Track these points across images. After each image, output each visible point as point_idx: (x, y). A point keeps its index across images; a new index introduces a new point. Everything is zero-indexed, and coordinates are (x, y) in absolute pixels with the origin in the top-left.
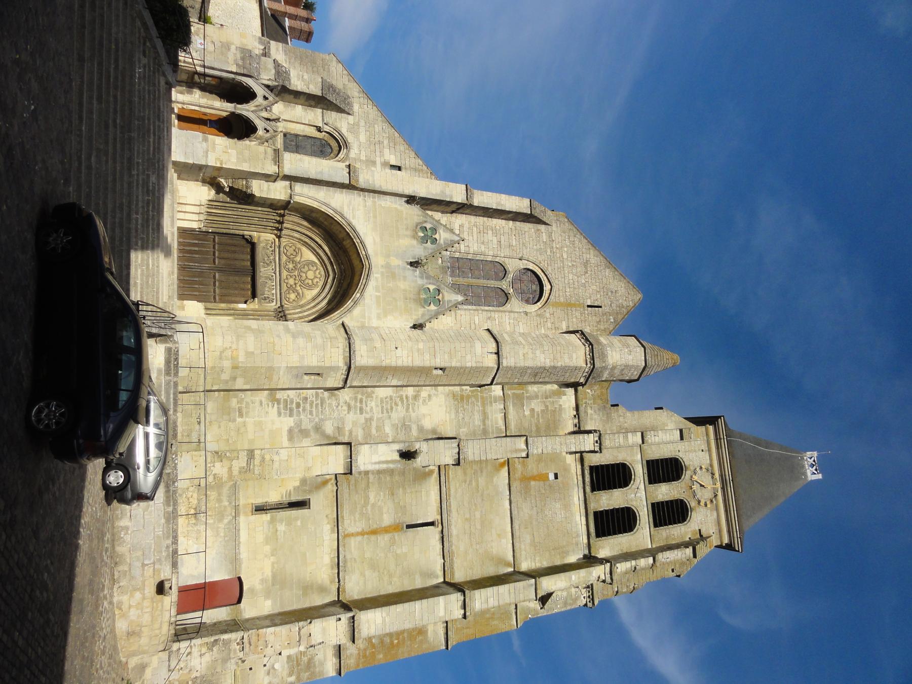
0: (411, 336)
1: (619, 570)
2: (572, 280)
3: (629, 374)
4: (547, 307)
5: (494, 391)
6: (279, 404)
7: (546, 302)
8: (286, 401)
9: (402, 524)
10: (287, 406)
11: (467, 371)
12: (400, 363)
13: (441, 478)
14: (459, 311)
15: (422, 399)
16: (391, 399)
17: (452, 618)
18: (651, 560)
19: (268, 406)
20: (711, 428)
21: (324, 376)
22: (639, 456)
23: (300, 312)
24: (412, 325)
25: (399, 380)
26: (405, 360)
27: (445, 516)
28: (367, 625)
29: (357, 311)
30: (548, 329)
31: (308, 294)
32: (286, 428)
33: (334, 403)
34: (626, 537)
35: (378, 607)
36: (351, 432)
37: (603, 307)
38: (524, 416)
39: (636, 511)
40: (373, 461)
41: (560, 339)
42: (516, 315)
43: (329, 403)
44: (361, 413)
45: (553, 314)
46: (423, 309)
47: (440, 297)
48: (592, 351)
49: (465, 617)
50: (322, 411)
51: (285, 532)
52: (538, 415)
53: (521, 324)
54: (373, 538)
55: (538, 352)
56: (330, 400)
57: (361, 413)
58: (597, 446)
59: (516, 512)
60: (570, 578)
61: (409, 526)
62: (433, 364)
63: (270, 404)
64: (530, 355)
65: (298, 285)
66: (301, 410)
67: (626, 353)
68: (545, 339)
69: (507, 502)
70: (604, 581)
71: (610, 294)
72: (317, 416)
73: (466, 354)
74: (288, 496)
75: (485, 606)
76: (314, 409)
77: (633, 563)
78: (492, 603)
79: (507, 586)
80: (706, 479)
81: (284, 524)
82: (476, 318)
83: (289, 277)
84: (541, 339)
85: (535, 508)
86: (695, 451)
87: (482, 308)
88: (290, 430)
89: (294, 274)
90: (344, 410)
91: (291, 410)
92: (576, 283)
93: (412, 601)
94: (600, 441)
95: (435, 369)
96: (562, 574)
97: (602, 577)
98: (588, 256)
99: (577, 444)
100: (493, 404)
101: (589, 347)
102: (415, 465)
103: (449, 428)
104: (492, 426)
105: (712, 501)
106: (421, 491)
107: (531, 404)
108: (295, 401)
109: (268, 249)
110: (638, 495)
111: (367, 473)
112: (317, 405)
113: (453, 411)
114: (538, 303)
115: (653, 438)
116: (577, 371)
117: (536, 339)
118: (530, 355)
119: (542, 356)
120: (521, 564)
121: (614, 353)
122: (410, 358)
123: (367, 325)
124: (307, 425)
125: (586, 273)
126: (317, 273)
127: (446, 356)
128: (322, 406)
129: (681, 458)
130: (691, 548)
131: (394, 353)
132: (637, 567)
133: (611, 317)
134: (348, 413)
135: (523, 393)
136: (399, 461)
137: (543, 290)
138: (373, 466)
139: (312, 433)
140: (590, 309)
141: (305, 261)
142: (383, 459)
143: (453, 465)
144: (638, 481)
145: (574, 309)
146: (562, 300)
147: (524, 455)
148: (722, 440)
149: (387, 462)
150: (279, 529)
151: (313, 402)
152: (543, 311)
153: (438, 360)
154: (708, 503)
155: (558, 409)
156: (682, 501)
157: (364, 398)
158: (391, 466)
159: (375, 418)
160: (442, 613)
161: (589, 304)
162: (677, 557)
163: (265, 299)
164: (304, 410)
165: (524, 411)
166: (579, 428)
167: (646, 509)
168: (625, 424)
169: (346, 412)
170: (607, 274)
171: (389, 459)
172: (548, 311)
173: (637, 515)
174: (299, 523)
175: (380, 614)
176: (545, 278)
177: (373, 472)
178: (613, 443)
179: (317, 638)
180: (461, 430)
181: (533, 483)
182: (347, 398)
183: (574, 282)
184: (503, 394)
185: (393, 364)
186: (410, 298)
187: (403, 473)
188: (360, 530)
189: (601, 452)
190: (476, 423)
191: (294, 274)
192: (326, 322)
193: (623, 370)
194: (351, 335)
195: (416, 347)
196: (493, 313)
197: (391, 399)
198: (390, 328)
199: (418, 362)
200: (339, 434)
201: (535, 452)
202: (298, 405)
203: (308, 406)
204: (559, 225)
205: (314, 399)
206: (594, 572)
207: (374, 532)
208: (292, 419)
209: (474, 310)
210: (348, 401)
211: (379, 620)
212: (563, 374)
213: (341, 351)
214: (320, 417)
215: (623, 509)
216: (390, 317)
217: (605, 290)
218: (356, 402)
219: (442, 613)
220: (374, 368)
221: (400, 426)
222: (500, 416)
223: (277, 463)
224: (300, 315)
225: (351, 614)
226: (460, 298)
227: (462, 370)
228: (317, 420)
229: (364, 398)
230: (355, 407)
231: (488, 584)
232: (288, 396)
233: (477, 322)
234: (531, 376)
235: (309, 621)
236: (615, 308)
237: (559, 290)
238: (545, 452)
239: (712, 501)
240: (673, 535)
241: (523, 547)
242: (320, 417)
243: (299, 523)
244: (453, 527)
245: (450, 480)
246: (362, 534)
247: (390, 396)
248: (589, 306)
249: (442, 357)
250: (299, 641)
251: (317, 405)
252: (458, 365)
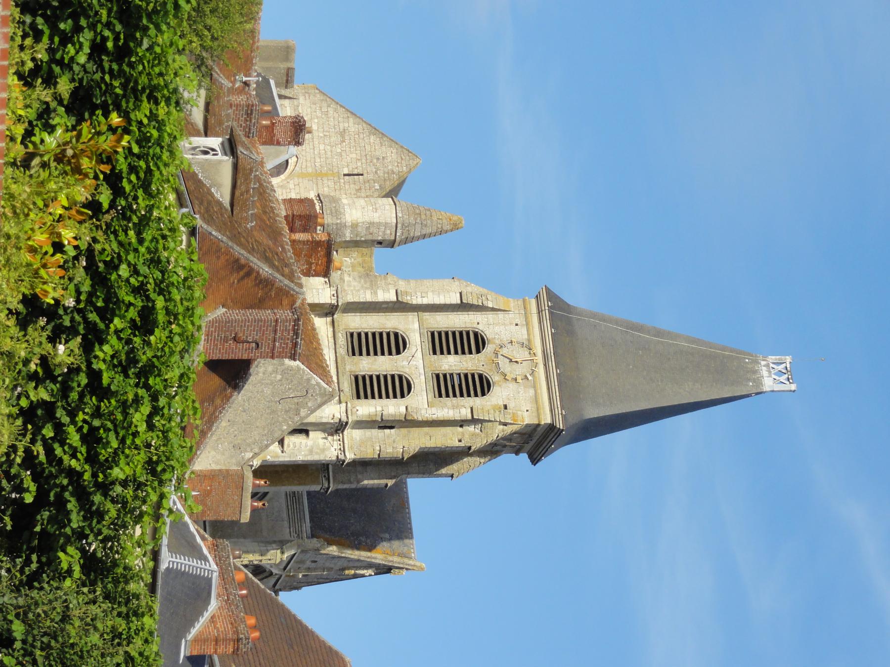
22: (416, 326)
37: (365, 175)
71: (375, 161)
92: (329, 153)
98: (346, 125)
133: (376, 184)
161: (346, 171)
172: (291, 182)
204: (307, 98)
237: (306, 161)
248: (345, 175)
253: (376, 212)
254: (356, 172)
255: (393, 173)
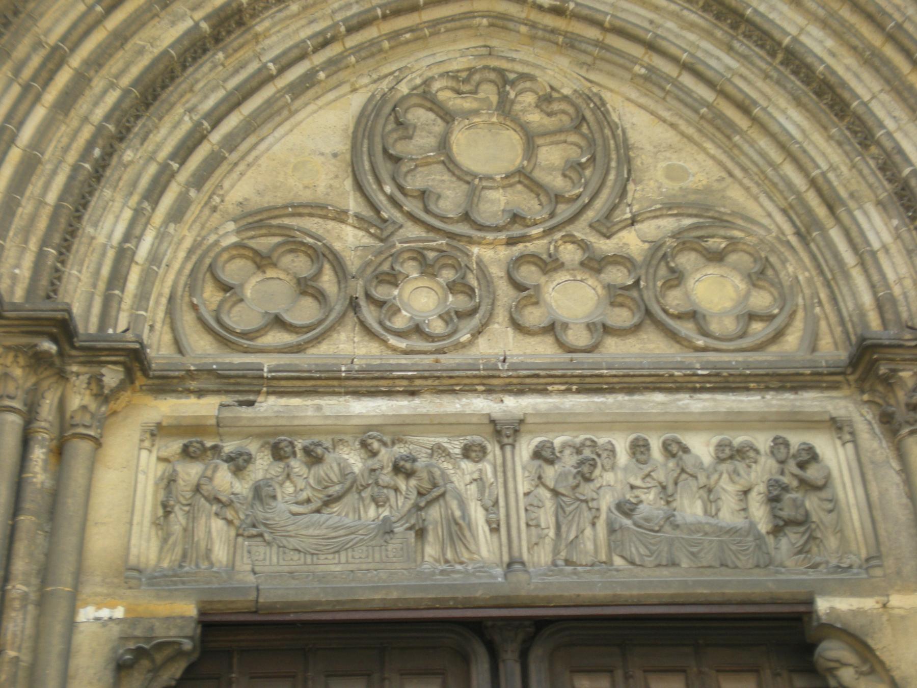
31: (673, 173)
65: (605, 246)
83: (533, 316)
89: (497, 272)
109: (262, 494)
126: (467, 104)
141: (359, 186)
163: (802, 522)
191: (497, 272)
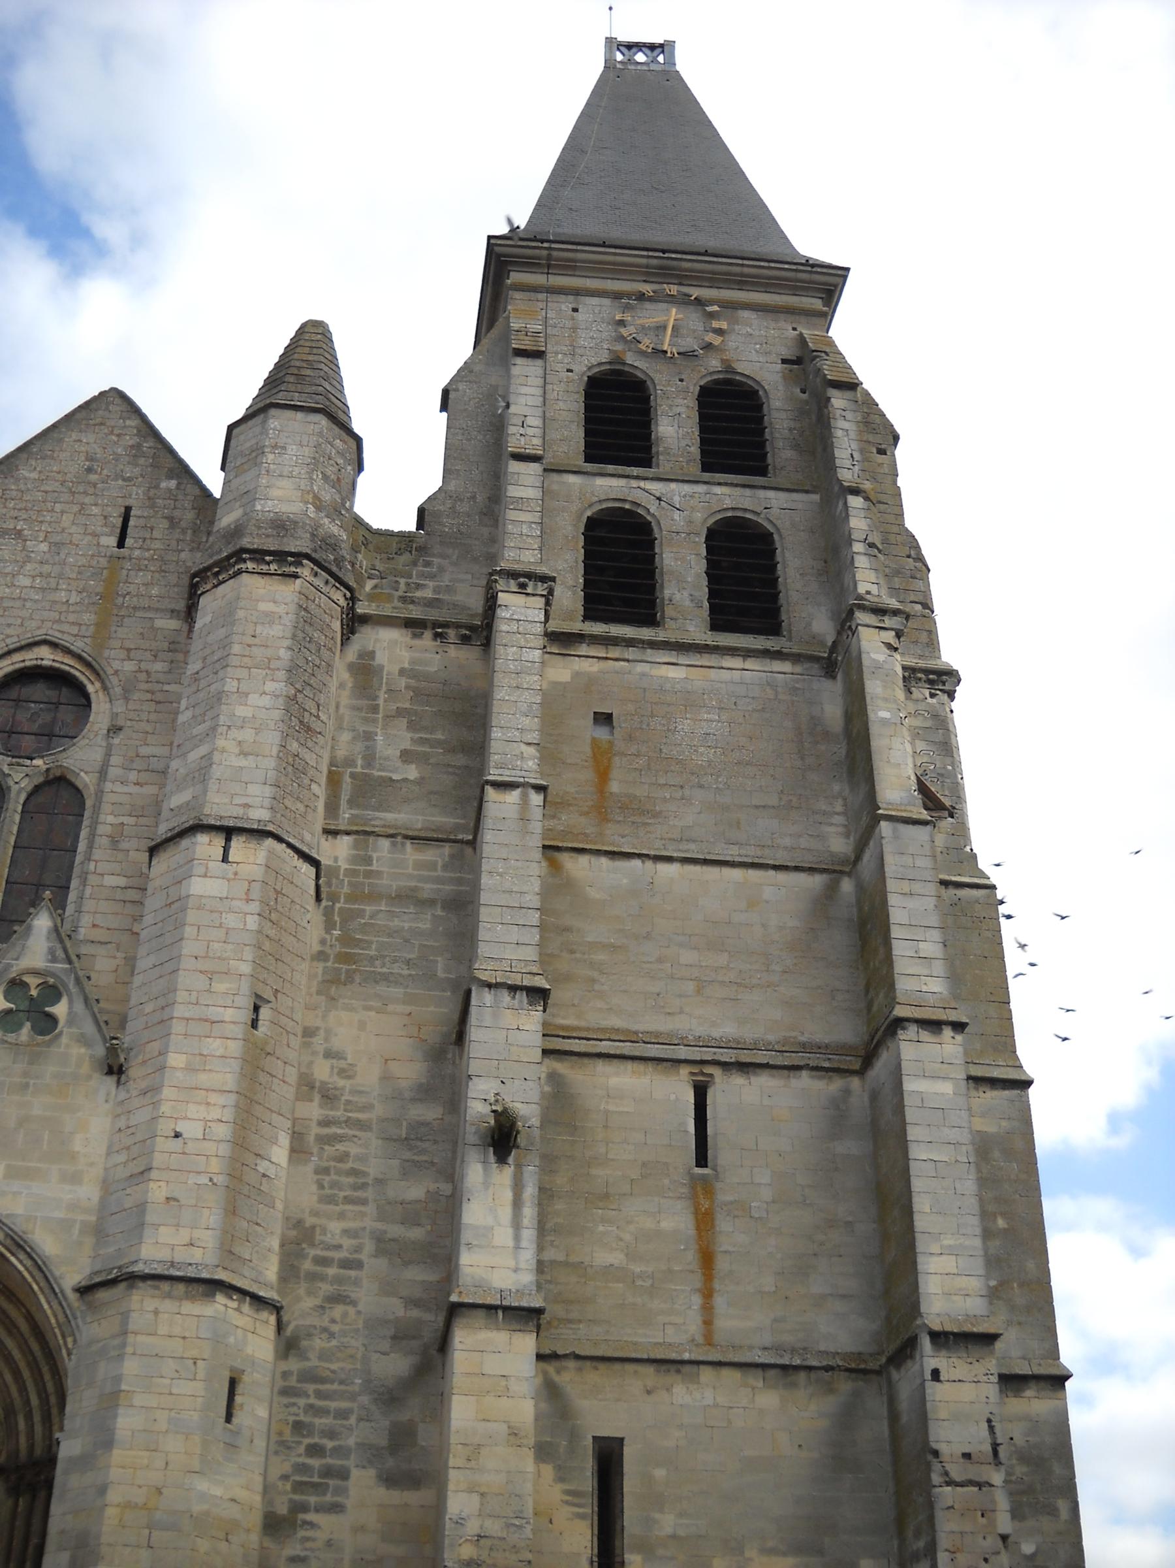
0: (143, 1085)
1: (874, 589)
2: (34, 577)
3: (341, 461)
4: (104, 663)
5: (336, 859)
6: (304, 1508)
7: (88, 665)
8: (299, 1487)
9: (693, 1177)
10: (315, 1486)
11: (272, 933)
12: (223, 1131)
13: (577, 1049)
14: (82, 931)
15: (336, 1078)
16: (326, 1171)
17: (960, 1060)
18: (855, 502)
19: (307, 1539)
20: (515, 277)
21: (238, 1364)
22: (572, 479)
23: (29, 1416)
24: (111, 1081)
25: (274, 1141)
26: (215, 1114)
27: (682, 1053)
28: (955, 1298)
29: (47, 1244)
30: (170, 672)
32: (382, 1493)
33: (318, 1343)
34: (787, 554)
35: (914, 1263)
36: (411, 1302)
38: (420, 782)
39: (719, 516)
40: (510, 1243)
41: (210, 639)
42: (114, 760)
43: (320, 1358)
44: (359, 1265)
45: (129, 650)
46: (64, 1040)
47: (33, 981)
48: (258, 555)
49: (959, 1027)
50: (342, 1382)
51: (681, 1515)
52: (422, 741)
53: (144, 751)
54: (722, 1264)
55: (241, 711)
56: (311, 1355)
57: (359, 1265)
58: (535, 586)
59: (692, 846)
60: (884, 722)
61: (702, 1158)
62: (238, 1031)
63: (301, 1533)
64: (247, 735)
66: (329, 1444)
67: (279, 460)
68: (203, 683)
69: (664, 868)
70: (899, 634)
71: (93, 477)
72: (353, 1397)
73: (221, 926)
74: (582, 1501)
75: (939, 968)
76: (333, 1405)
77: (858, 547)
78: (931, 947)
79: (893, 900)
80: (652, 315)
81: (657, 1516)
82: (110, 881)
84: (201, 695)
85: (687, 792)
86: (574, 329)
87: (79, 859)
88: (387, 1480)
90: (345, 1315)
91: (328, 1472)
92: (46, 569)
93: (906, 1170)
94: (523, 579)
95: (254, 1024)
96: (875, 743)
97: (889, 636)
99: (523, 644)
100: (374, 867)
101: (245, 561)
102: (535, 1121)
103: (432, 1009)
104: (438, 880)
105: (712, 316)
106: (607, 1112)
107: (387, 759)
108: (301, 1460)
110: (676, 500)
111: (541, 1267)
112: (319, 1395)
113: (381, 989)
114: (90, 688)
115: (530, 431)
116: (312, 607)
117: (198, 711)
118: (247, 735)
119: (254, 699)
120: (832, 854)
121: (275, 493)
122: (213, 1098)
123: (94, 1218)
124: (376, 1431)
125: (19, 534)
127: (220, 986)
128: (323, 1380)
129: (590, 368)
130: (832, 392)
131: (190, 1144)
132: (870, 540)
133: (163, 485)
134: (354, 1303)
135: (353, 775)
136: (519, 1167)
137: (51, 668)
138: (524, 1244)
139: (404, 1416)
140: (129, 542)
142: (506, 1213)
143: (544, 1011)
144: (638, 496)
145: (123, 588)
146: (88, 617)
147: (536, 799)
148: (555, 253)
149: (517, 1203)
150: (669, 1530)
151: (311, 1406)
152: (114, 680)
153: (229, 1014)
154: (715, 324)
155: (413, 682)
156: (703, 389)
157: (312, 1252)
158: (530, 1191)
159: (379, 1226)
160: (947, 1088)
161: (112, 541)
162: (852, 435)
164: (331, 1434)
165: (405, 780)
166: (472, 628)
167: (718, 490)
168: (479, 498)
169: (351, 1310)
170: (34, 475)
171: (508, 1195)
173: (730, 514)
174: (660, 1473)
175: (935, 1259)
176: (17, 657)
177: (540, 1248)
178: (530, 540)
179: (976, 1438)
180: (441, 974)
181: (614, 787)
182: (309, 1303)
183: (41, 575)
184: (348, 833)
185: (224, 1150)
186: (26, 1074)
187: (549, 1163)
188: (697, 1300)
189: (553, 579)
190: (425, 925)
192: (70, 1340)
193: (325, 477)
194: (120, 1268)
195: (179, 1074)
196: (101, 829)
197: (326, 1171)
198: (109, 1147)
199: (226, 1076)
200: (414, 1338)
201: (531, 764)
202: (315, 1450)
203: (320, 1422)
205: (302, 1402)
206: (873, 656)
207: (707, 1259)
208: (355, 1473)
209: (84, 882)
210: (318, 1302)
211: (947, 1263)
212: (313, 647)
213: (168, 1305)
214: (357, 1388)
215: (709, 550)
216: (77, 1145)
217: (81, 489)
218: (323, 1278)
219: (947, 1088)
220: (231, 1211)
221: (408, 1155)
222: (411, 855)
223: (488, 1523)
224: (37, 1418)
225: (926, 1343)
226: (42, 922)
227: (267, 946)
228: (365, 1399)
229: (312, 1252)
230: (338, 1280)
231: (882, 950)
232: (285, 1477)
233: (122, 881)
234: (310, 744)
235: (930, 1457)
236: (137, 470)
237: (59, 621)
238: (534, 737)
239: (712, 316)
240: (790, 430)
241: (787, 841)
242: (357, 1388)
243: (660, 1473)
244: (716, 1033)
245: (583, 1024)
246: (708, 1294)
247: (317, 1172)
248: (121, 544)
249: (221, 1002)
250: (979, 1485)
251: (319, 1395)
252: (248, 954)
253: (284, 448)
254: (119, 522)
255: (138, 446)
